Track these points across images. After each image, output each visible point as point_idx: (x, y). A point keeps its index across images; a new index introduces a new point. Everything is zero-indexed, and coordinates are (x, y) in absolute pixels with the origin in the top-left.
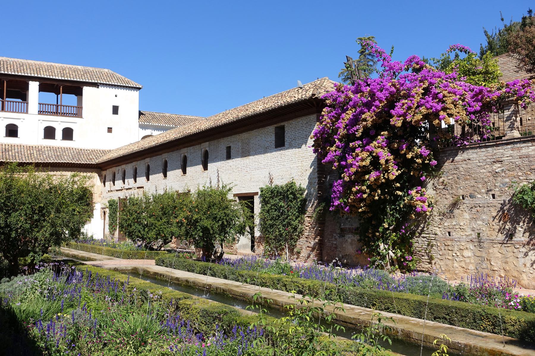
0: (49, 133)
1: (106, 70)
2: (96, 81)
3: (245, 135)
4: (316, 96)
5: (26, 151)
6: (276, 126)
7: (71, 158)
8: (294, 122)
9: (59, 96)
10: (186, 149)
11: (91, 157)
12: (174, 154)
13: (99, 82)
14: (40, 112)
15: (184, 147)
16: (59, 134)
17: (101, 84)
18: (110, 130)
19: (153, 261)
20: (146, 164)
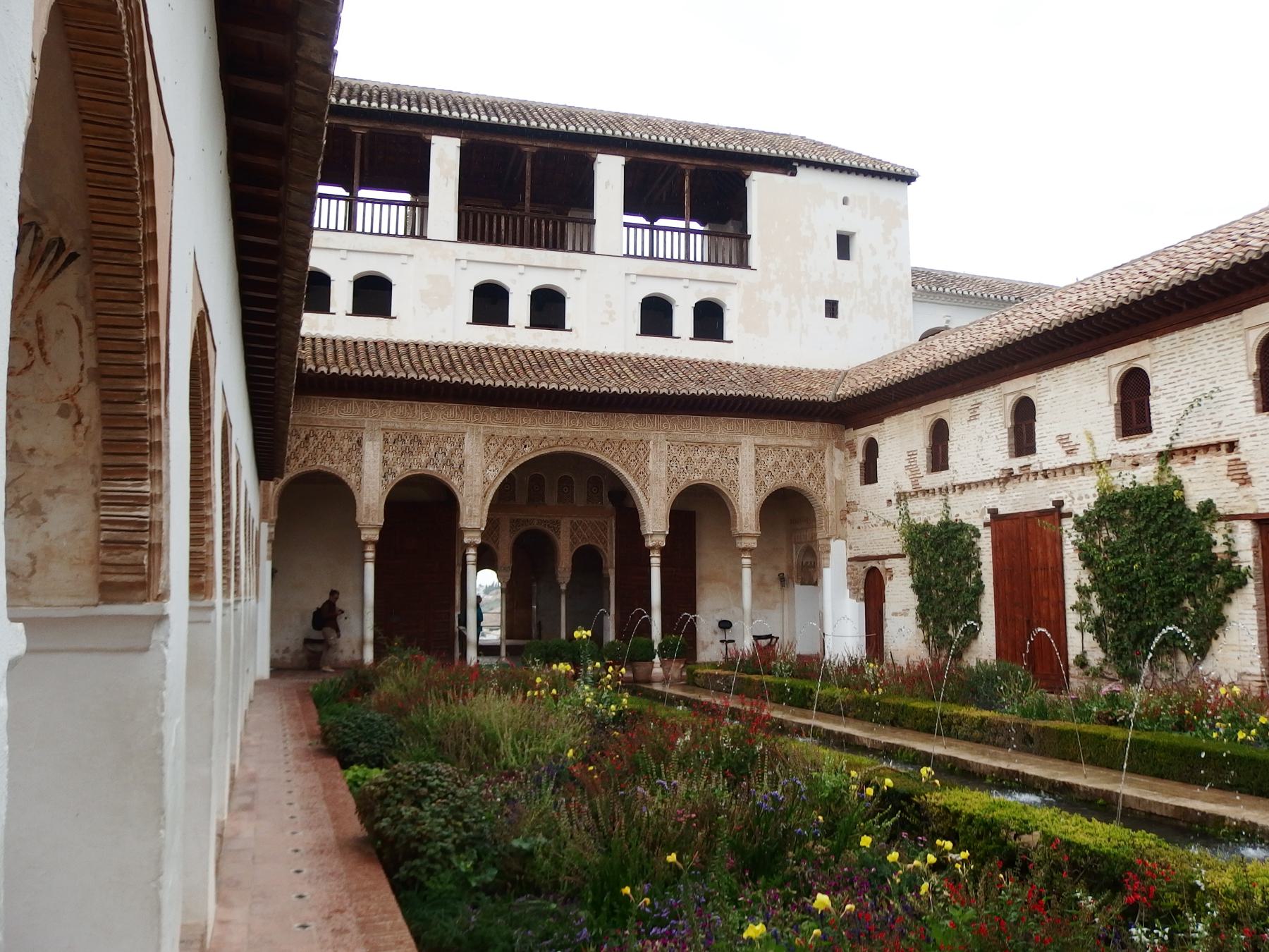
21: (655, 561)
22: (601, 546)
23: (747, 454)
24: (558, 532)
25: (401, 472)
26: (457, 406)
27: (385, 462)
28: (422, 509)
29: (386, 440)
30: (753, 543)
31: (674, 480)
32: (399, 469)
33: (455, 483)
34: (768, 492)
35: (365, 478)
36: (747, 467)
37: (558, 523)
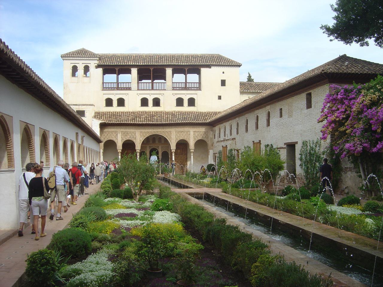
0: (180, 102)
3: (290, 100)
4: (325, 71)
5: (165, 115)
6: (306, 93)
11: (206, 118)
14: (174, 89)
15: (257, 109)
16: (186, 103)
18: (220, 98)
21: (173, 154)
22: (168, 151)
23: (192, 133)
24: (159, 149)
25: (125, 139)
26: (134, 127)
27: (122, 138)
28: (129, 146)
29: (122, 134)
30: (193, 151)
31: (177, 139)
32: (124, 139)
33: (134, 141)
34: (196, 141)
35: (118, 141)
36: (192, 136)
37: (159, 147)
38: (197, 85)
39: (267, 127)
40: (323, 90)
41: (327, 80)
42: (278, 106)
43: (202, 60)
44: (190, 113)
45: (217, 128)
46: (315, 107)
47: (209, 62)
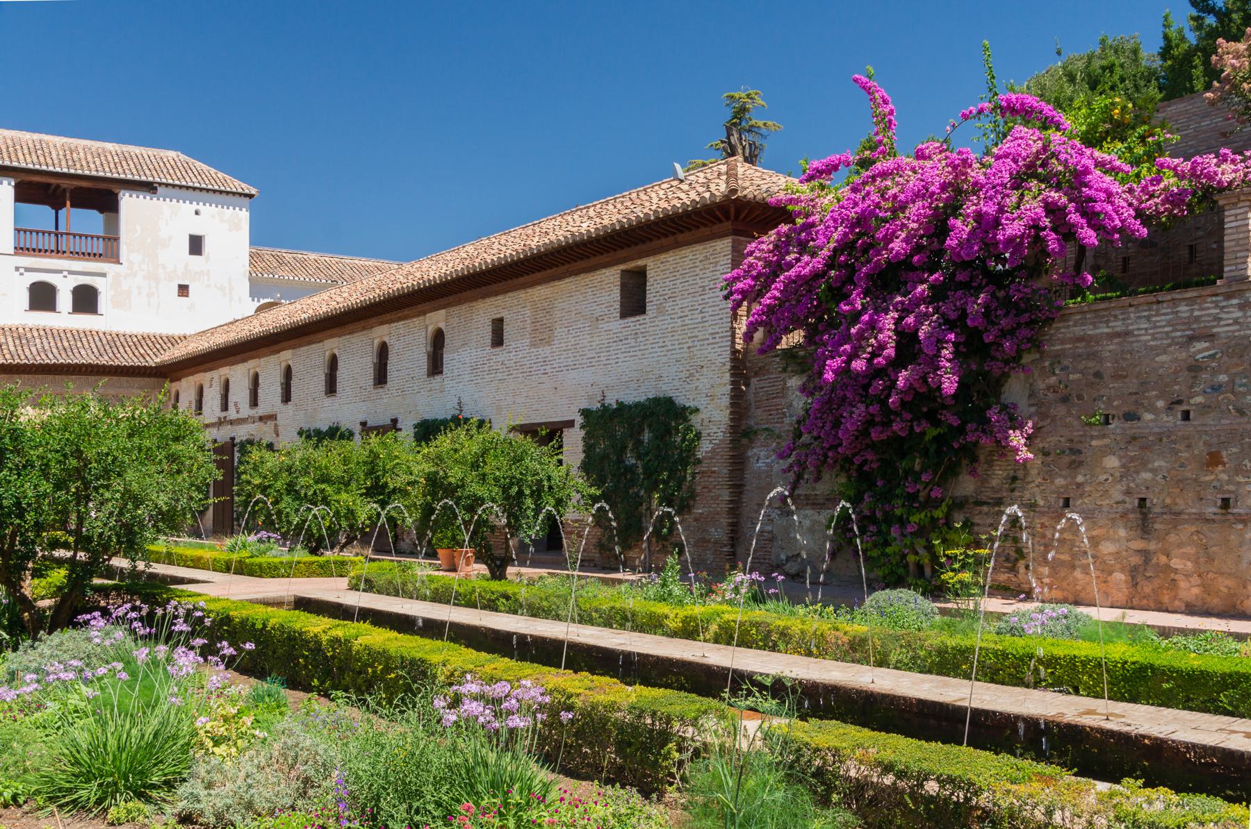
0: (42, 297)
1: (172, 154)
2: (151, 179)
3: (540, 293)
6: (622, 267)
7: (97, 354)
8: (670, 258)
9: (62, 212)
10: (386, 327)
12: (353, 340)
13: (158, 180)
14: (20, 250)
15: (382, 323)
16: (65, 300)
17: (160, 184)
18: (183, 290)
19: (344, 582)
20: (284, 365)
38: (99, 247)
39: (429, 376)
40: (701, 257)
41: (728, 225)
42: (483, 311)
43: (124, 163)
44: (82, 335)
45: (186, 387)
46: (661, 310)
47: (148, 172)
